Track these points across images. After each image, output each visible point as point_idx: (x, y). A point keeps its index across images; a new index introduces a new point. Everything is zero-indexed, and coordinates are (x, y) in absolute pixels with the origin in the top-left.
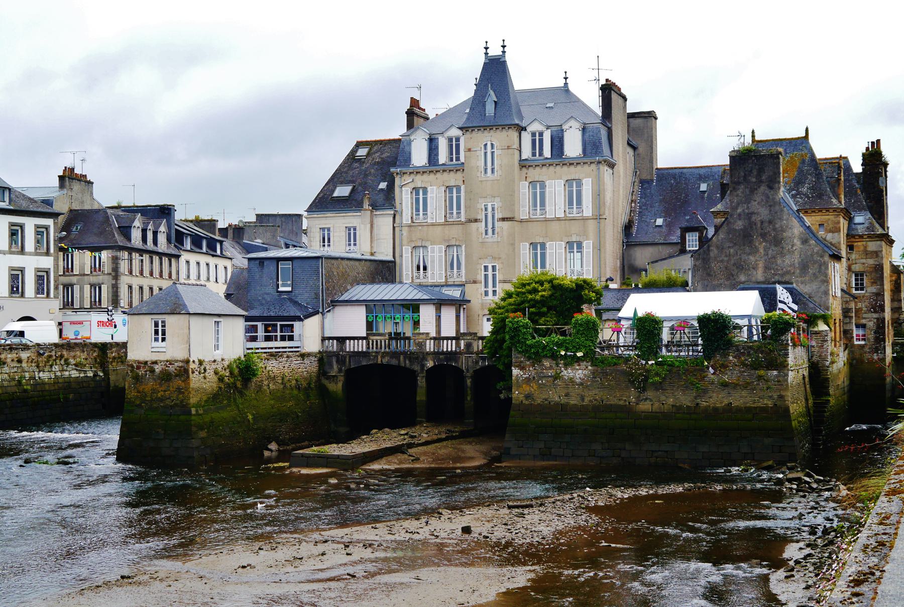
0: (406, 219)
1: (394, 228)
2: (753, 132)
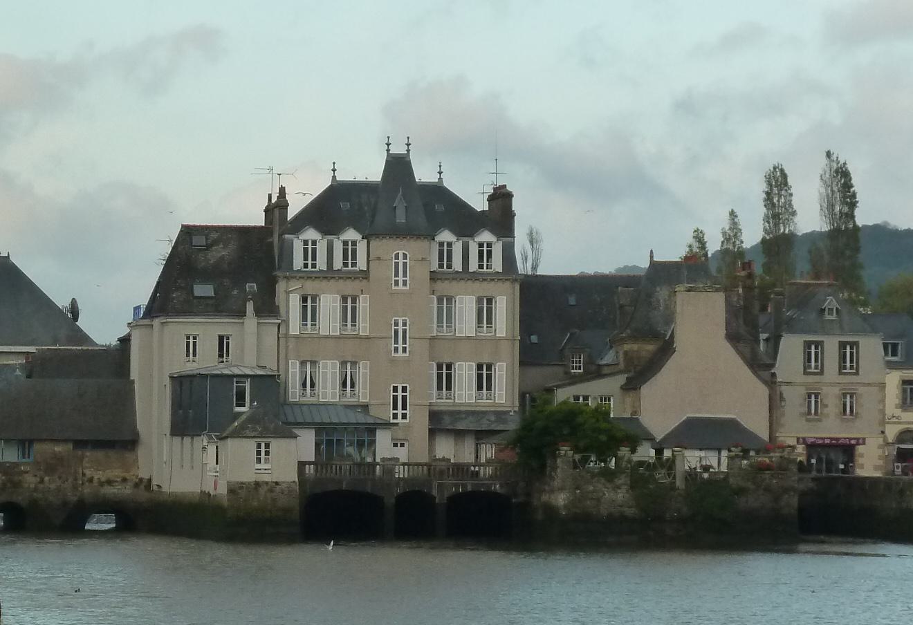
0: (294, 327)
1: (278, 338)
2: (651, 251)
